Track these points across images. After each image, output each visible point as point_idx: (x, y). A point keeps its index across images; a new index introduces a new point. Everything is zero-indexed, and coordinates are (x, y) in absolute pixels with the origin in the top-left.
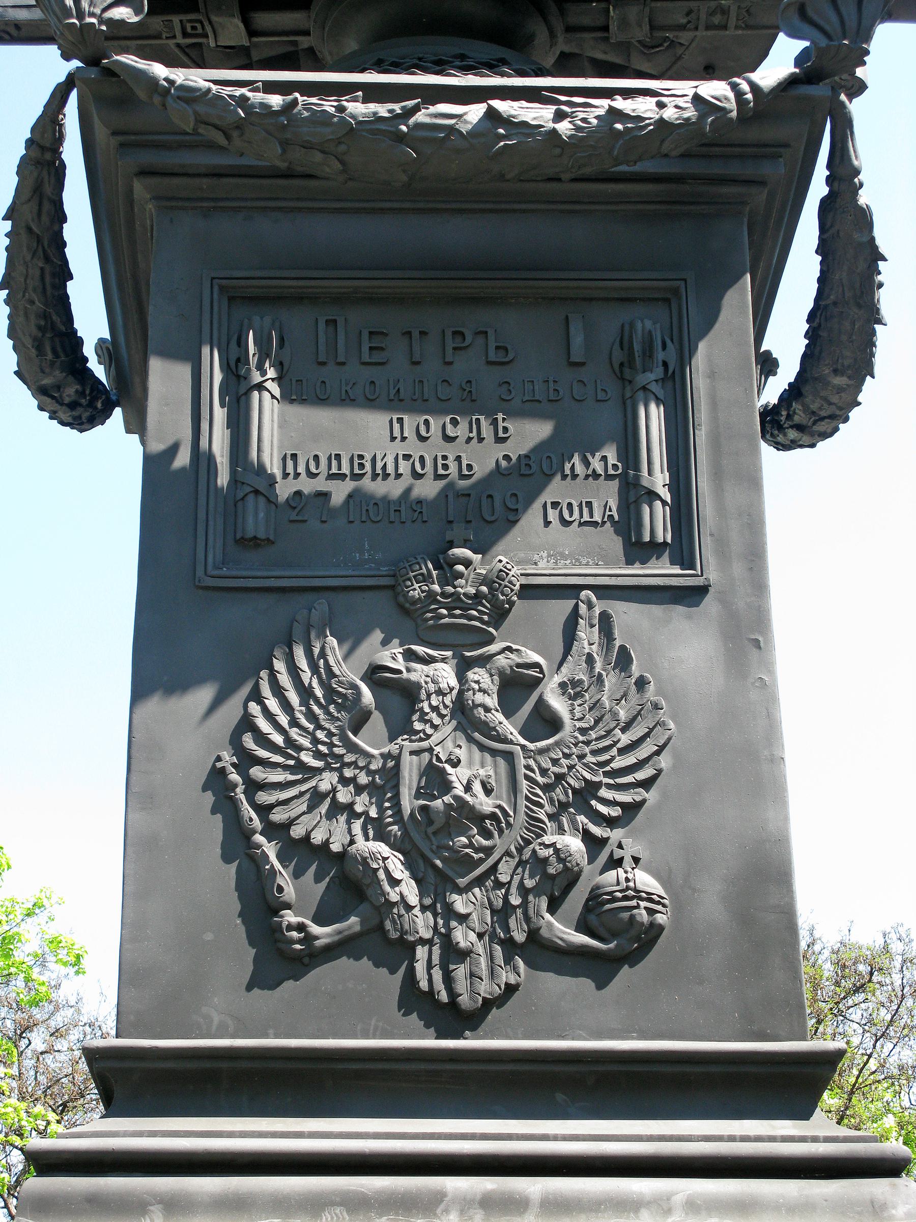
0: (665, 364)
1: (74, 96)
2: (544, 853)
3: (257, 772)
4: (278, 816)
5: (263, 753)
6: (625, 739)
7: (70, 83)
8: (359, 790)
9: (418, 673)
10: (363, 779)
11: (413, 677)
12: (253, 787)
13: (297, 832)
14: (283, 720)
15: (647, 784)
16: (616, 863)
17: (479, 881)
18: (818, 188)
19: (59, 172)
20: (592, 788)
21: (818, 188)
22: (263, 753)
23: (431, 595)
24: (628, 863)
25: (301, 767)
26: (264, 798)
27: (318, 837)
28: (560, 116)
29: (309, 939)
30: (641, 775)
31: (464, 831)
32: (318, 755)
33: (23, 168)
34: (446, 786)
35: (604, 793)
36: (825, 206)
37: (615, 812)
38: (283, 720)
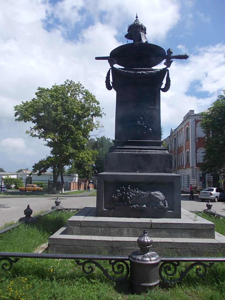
1: (111, 69)
7: (111, 68)
18: (166, 76)
19: (110, 74)
21: (166, 76)
28: (147, 73)
33: (107, 74)
36: (167, 78)
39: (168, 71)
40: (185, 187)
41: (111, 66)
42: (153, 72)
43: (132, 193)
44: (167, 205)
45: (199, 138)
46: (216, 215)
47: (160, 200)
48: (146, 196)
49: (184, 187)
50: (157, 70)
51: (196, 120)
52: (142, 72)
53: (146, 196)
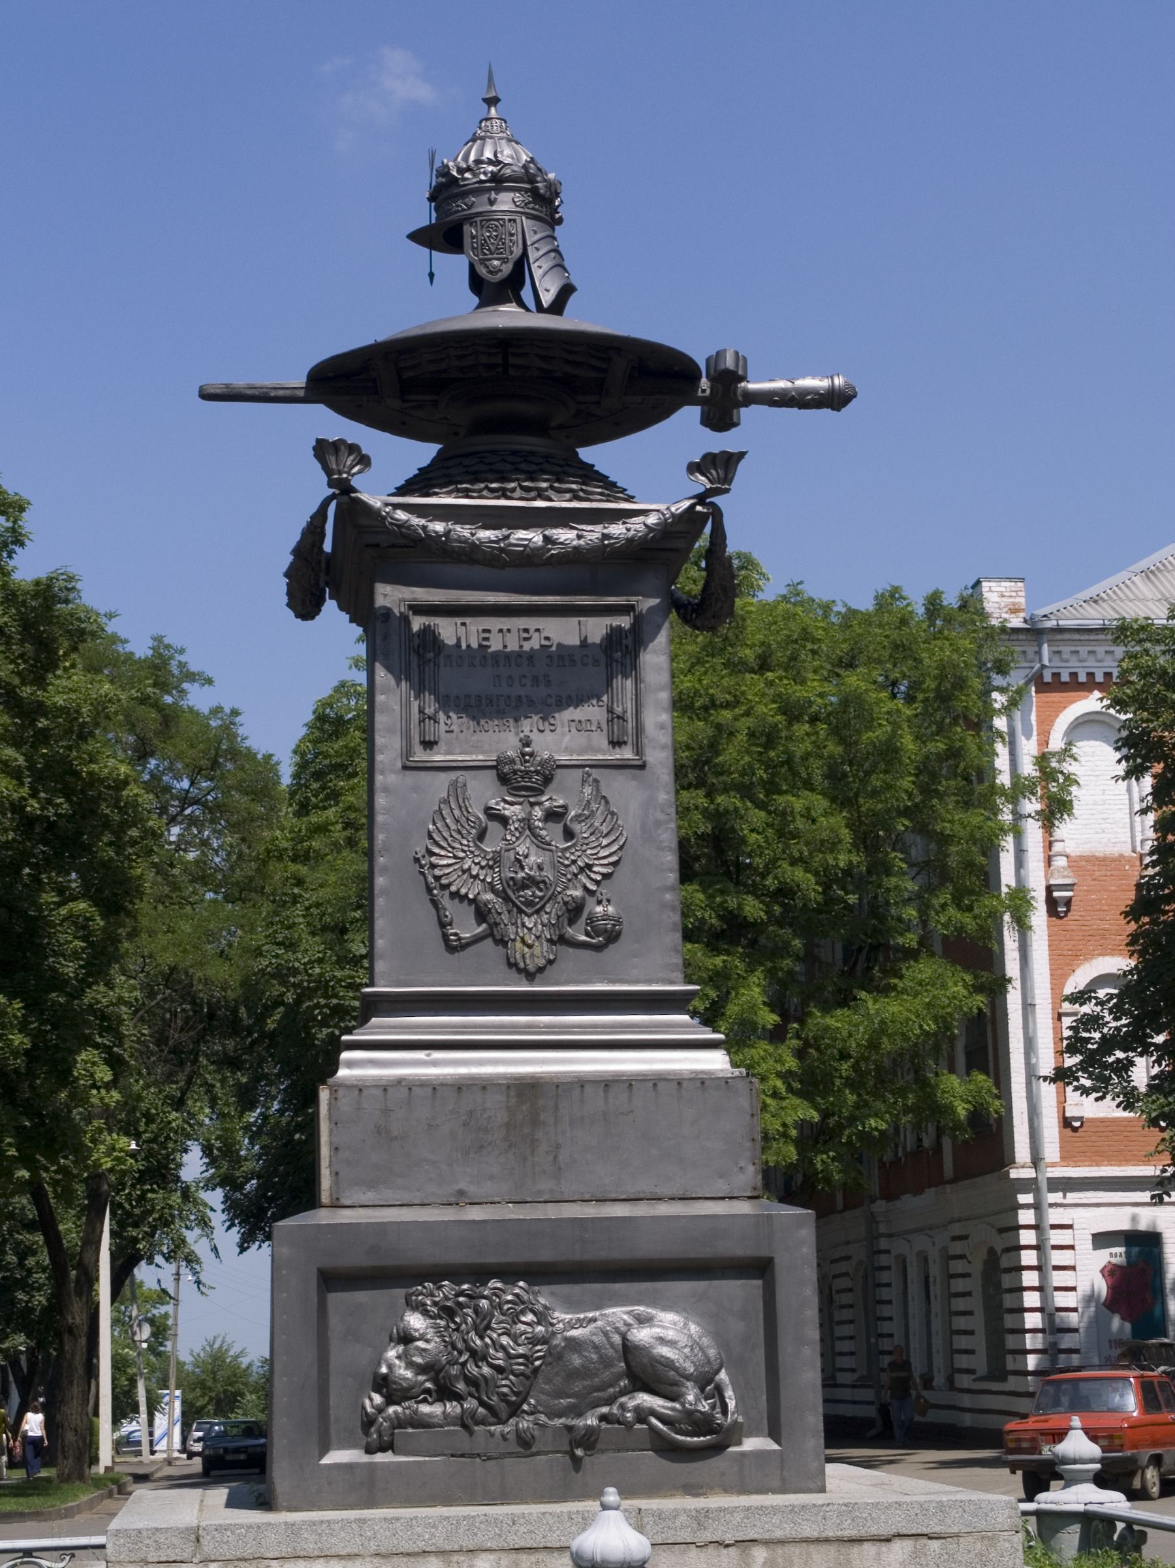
0: (627, 647)
1: (333, 505)
2: (566, 899)
3: (433, 859)
4: (444, 881)
5: (437, 850)
6: (605, 842)
7: (333, 496)
8: (482, 868)
9: (509, 810)
10: (484, 863)
11: (507, 813)
12: (433, 866)
13: (453, 888)
14: (446, 834)
15: (614, 864)
16: (599, 902)
17: (537, 912)
20: (589, 867)
22: (437, 850)
23: (515, 772)
24: (605, 903)
25: (455, 857)
26: (437, 872)
27: (463, 891)
29: (460, 939)
30: (614, 859)
31: (528, 887)
32: (464, 851)
34: (522, 868)
35: (595, 869)
37: (599, 878)
38: (446, 834)
39: (717, 514)
40: (964, 1381)
41: (331, 484)
42: (617, 529)
43: (505, 1340)
44: (731, 1404)
45: (1075, 863)
46: (1120, 1526)
47: (688, 1378)
48: (594, 1356)
49: (951, 1384)
50: (641, 519)
51: (1048, 678)
52: (551, 532)
53: (594, 1356)
